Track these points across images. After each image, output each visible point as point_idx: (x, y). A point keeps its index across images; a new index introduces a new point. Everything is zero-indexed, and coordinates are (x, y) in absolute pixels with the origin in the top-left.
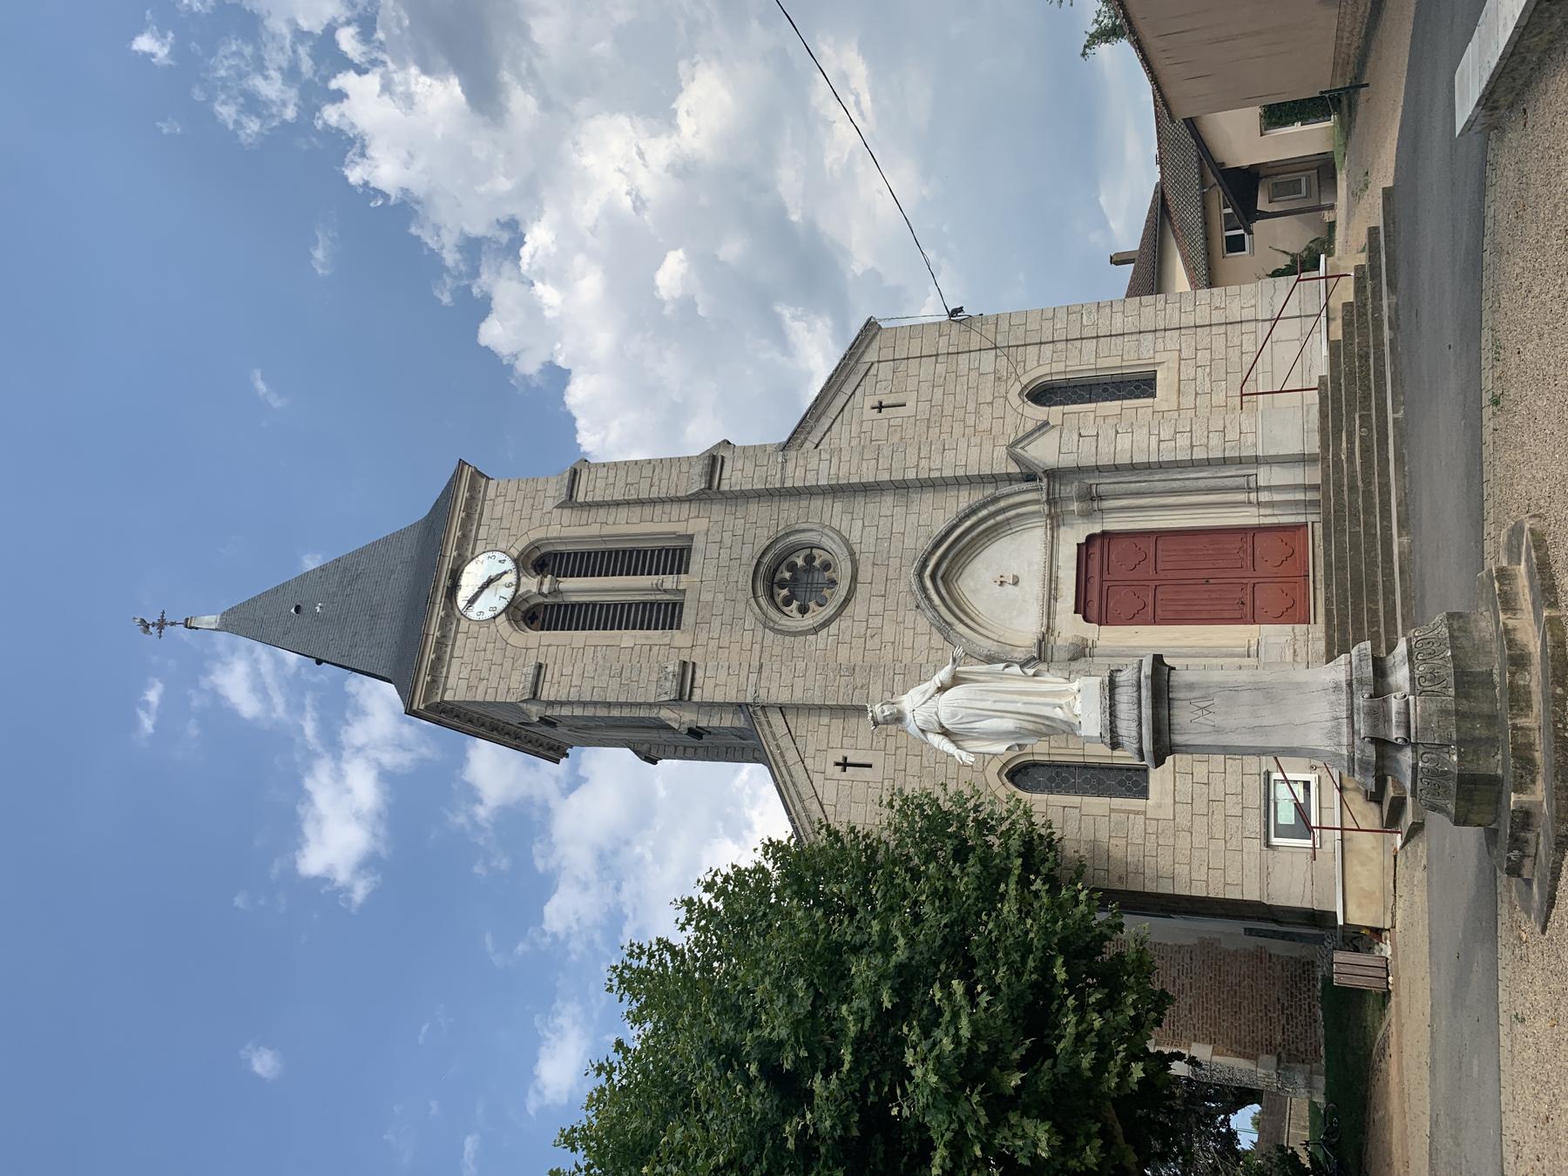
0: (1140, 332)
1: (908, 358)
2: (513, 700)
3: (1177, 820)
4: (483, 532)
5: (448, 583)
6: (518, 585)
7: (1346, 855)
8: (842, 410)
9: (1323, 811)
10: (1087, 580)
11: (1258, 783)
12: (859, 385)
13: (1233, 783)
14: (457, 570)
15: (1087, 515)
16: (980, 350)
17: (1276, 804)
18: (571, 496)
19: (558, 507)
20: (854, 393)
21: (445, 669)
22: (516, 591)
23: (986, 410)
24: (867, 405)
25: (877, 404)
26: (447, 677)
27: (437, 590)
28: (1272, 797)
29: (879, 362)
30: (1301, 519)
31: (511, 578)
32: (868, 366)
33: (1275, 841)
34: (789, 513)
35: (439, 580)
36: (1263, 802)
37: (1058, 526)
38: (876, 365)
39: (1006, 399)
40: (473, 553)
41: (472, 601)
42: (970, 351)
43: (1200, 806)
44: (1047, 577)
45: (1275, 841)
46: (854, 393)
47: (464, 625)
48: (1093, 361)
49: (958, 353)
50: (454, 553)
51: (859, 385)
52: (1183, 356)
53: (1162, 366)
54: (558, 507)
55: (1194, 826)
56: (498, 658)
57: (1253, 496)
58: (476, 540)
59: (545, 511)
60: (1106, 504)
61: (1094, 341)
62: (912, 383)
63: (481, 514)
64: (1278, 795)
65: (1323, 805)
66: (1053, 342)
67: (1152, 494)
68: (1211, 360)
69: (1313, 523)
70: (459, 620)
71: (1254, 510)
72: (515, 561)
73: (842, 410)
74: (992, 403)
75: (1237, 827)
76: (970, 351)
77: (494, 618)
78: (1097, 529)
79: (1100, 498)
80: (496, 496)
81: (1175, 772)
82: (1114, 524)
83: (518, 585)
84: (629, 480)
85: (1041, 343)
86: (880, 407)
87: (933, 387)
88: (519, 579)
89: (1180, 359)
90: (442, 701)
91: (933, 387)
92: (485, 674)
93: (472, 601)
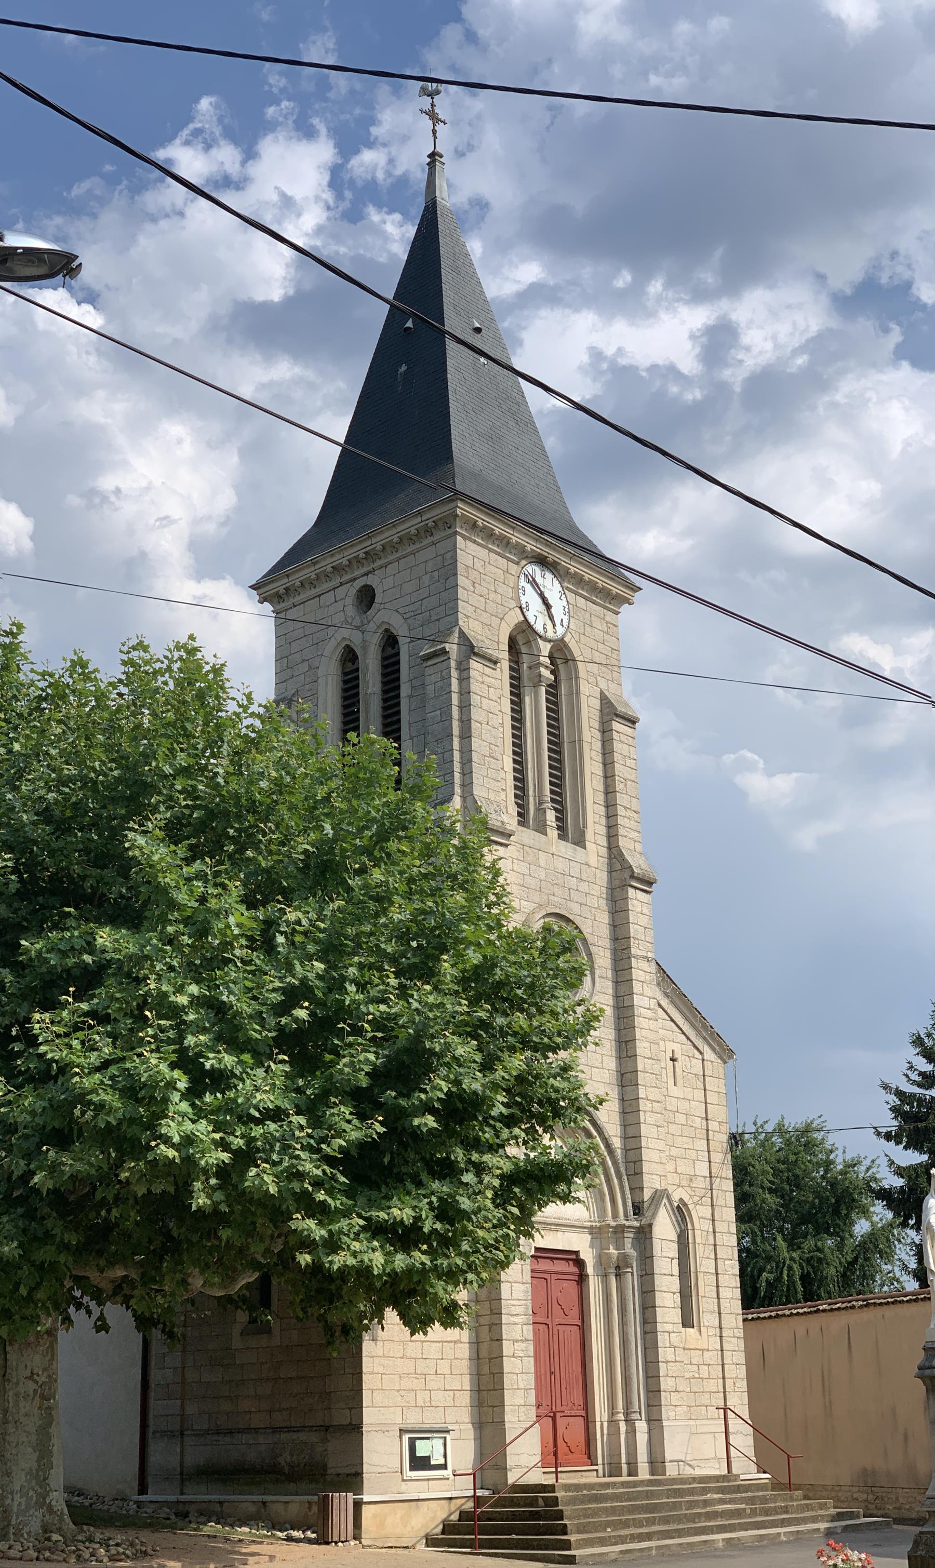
0: (720, 1314)
1: (705, 1090)
2: (461, 622)
3: (411, 1344)
4: (581, 602)
5: (550, 558)
6: (546, 640)
7: (407, 1504)
8: (672, 1020)
9: (426, 1482)
10: (552, 1259)
11: (439, 1421)
12: (688, 1038)
13: (438, 1398)
14: (555, 568)
15: (601, 1260)
16: (710, 1162)
17: (428, 1438)
18: (617, 715)
19: (602, 692)
20: (683, 1033)
21: (480, 541)
22: (540, 637)
23: (670, 1167)
24: (677, 1047)
25: (676, 1056)
26: (475, 542)
27: (547, 545)
28: (435, 1435)
29: (703, 1060)
30: (600, 1461)
31: (550, 634)
32: (701, 1049)
33: (406, 1438)
34: (603, 959)
35: (554, 550)
36: (428, 1426)
37: (591, 1234)
38: (700, 1057)
39: (679, 1186)
40: (567, 588)
41: (534, 583)
42: (709, 1152)
43: (421, 1367)
44: (561, 1222)
45: (406, 1438)
46: (683, 1033)
47: (514, 568)
48: (702, 1269)
49: (708, 1140)
50: (572, 570)
51: (688, 1038)
52: (705, 1353)
53: (698, 1333)
54: (602, 692)
55: (407, 1361)
56: (491, 606)
57: (621, 1416)
58: (576, 593)
59: (599, 678)
60: (613, 1279)
61: (714, 1271)
62: (688, 1092)
63: (594, 603)
64: (435, 1440)
65: (430, 1482)
66: (714, 1232)
67: (623, 1323)
68: (702, 1379)
69: (597, 1470)
70: (517, 563)
71: (605, 1417)
72: (562, 640)
73: (672, 1020)
74: (676, 1172)
75: (408, 1402)
76: (709, 1152)
77: (521, 608)
78: (590, 1270)
79: (617, 1275)
80: (607, 622)
81: (443, 1342)
82: (594, 1284)
83: (546, 640)
84: (629, 783)
85: (713, 1220)
86: (673, 1060)
87: (686, 1114)
88: (550, 641)
89: (703, 1350)
90: (456, 533)
91: (686, 1114)
92: (478, 589)
93: (534, 583)
